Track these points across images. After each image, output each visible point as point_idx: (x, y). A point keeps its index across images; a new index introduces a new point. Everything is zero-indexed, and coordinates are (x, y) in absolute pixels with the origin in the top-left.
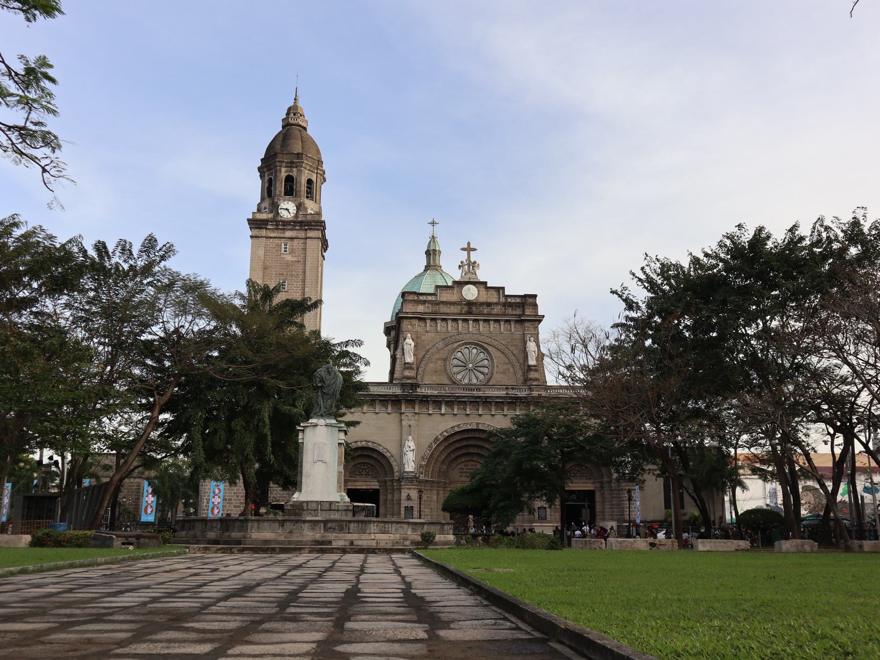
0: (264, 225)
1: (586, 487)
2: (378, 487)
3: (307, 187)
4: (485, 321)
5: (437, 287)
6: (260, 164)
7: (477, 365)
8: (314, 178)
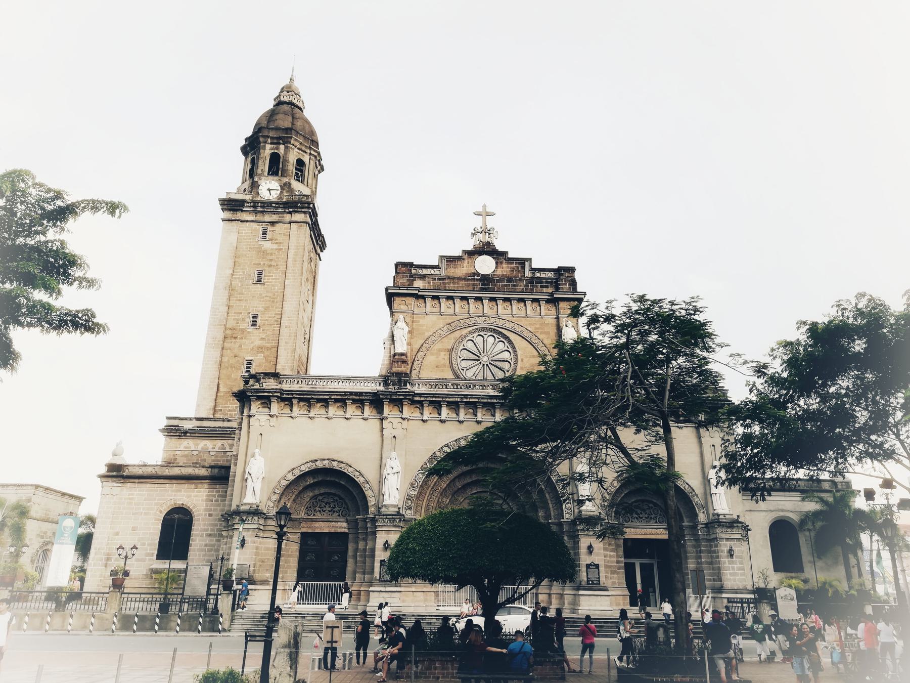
0: (240, 206)
1: (657, 534)
2: (346, 530)
3: (296, 169)
4: (506, 300)
5: (442, 257)
6: (243, 143)
7: (494, 358)
8: (306, 159)
